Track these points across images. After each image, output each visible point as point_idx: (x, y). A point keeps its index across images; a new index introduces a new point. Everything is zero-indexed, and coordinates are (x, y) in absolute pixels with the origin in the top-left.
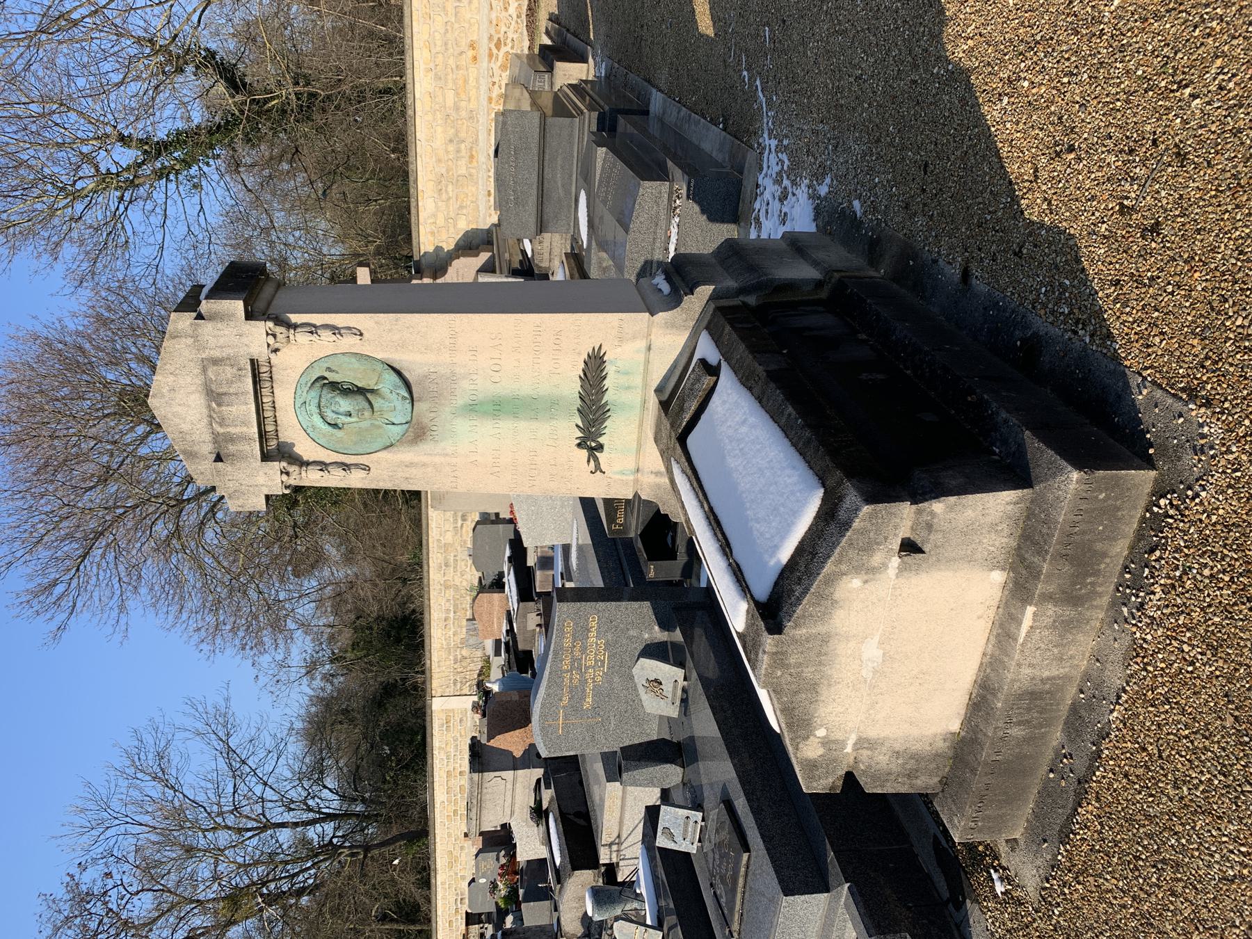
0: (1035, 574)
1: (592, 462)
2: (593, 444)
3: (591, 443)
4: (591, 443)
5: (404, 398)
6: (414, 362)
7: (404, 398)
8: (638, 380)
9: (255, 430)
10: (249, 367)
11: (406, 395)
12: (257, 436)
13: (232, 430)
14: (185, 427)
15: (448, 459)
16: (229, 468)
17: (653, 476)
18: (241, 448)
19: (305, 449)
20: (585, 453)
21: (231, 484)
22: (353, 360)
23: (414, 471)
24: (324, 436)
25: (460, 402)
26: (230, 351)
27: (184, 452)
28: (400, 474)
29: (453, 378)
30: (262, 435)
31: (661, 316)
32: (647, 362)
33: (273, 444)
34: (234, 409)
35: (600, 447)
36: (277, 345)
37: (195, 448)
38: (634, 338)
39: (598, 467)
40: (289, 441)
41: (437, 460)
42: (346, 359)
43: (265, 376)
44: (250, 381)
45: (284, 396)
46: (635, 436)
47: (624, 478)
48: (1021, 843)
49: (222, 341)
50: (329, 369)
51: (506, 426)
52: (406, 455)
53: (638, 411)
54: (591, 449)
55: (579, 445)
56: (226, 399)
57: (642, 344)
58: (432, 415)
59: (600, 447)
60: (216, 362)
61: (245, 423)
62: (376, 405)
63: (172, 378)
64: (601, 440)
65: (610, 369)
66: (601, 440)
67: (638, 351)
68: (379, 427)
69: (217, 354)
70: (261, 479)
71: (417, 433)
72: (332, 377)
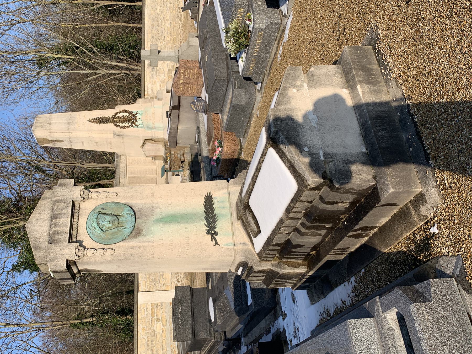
0: (353, 78)
1: (214, 240)
2: (213, 232)
3: (212, 231)
4: (212, 231)
5: (132, 215)
6: (137, 203)
7: (132, 215)
8: (227, 204)
9: (69, 229)
10: (71, 203)
11: (133, 214)
12: (69, 231)
13: (58, 229)
14: (38, 235)
15: (150, 244)
16: (53, 247)
17: (241, 245)
18: (61, 237)
19: (88, 242)
20: (210, 236)
21: (52, 254)
22: (113, 204)
23: (135, 251)
24: (97, 236)
25: (155, 218)
26: (65, 197)
27: (34, 247)
28: (128, 252)
29: (153, 208)
30: (71, 234)
31: (231, 181)
32: (230, 199)
33: (74, 240)
34: (61, 220)
35: (216, 233)
36: (84, 196)
37: (40, 245)
38: (222, 189)
39: (216, 243)
40: (81, 240)
41: (145, 244)
42: (110, 204)
43: (76, 210)
44: (70, 208)
45: (82, 221)
46: (230, 228)
47: (229, 247)
48: (424, 191)
49: (63, 193)
50: (103, 208)
51: (174, 227)
52: (132, 243)
53: (229, 216)
54: (212, 235)
55: (208, 233)
56: (59, 216)
57: (226, 191)
58: (144, 224)
59: (216, 233)
60: (58, 201)
61: (65, 226)
62: (120, 220)
63: (38, 215)
64: (215, 230)
65: (215, 201)
66: (215, 230)
67: (225, 194)
68: (121, 231)
69: (60, 198)
70: (66, 251)
71: (136, 232)
72: (103, 211)
